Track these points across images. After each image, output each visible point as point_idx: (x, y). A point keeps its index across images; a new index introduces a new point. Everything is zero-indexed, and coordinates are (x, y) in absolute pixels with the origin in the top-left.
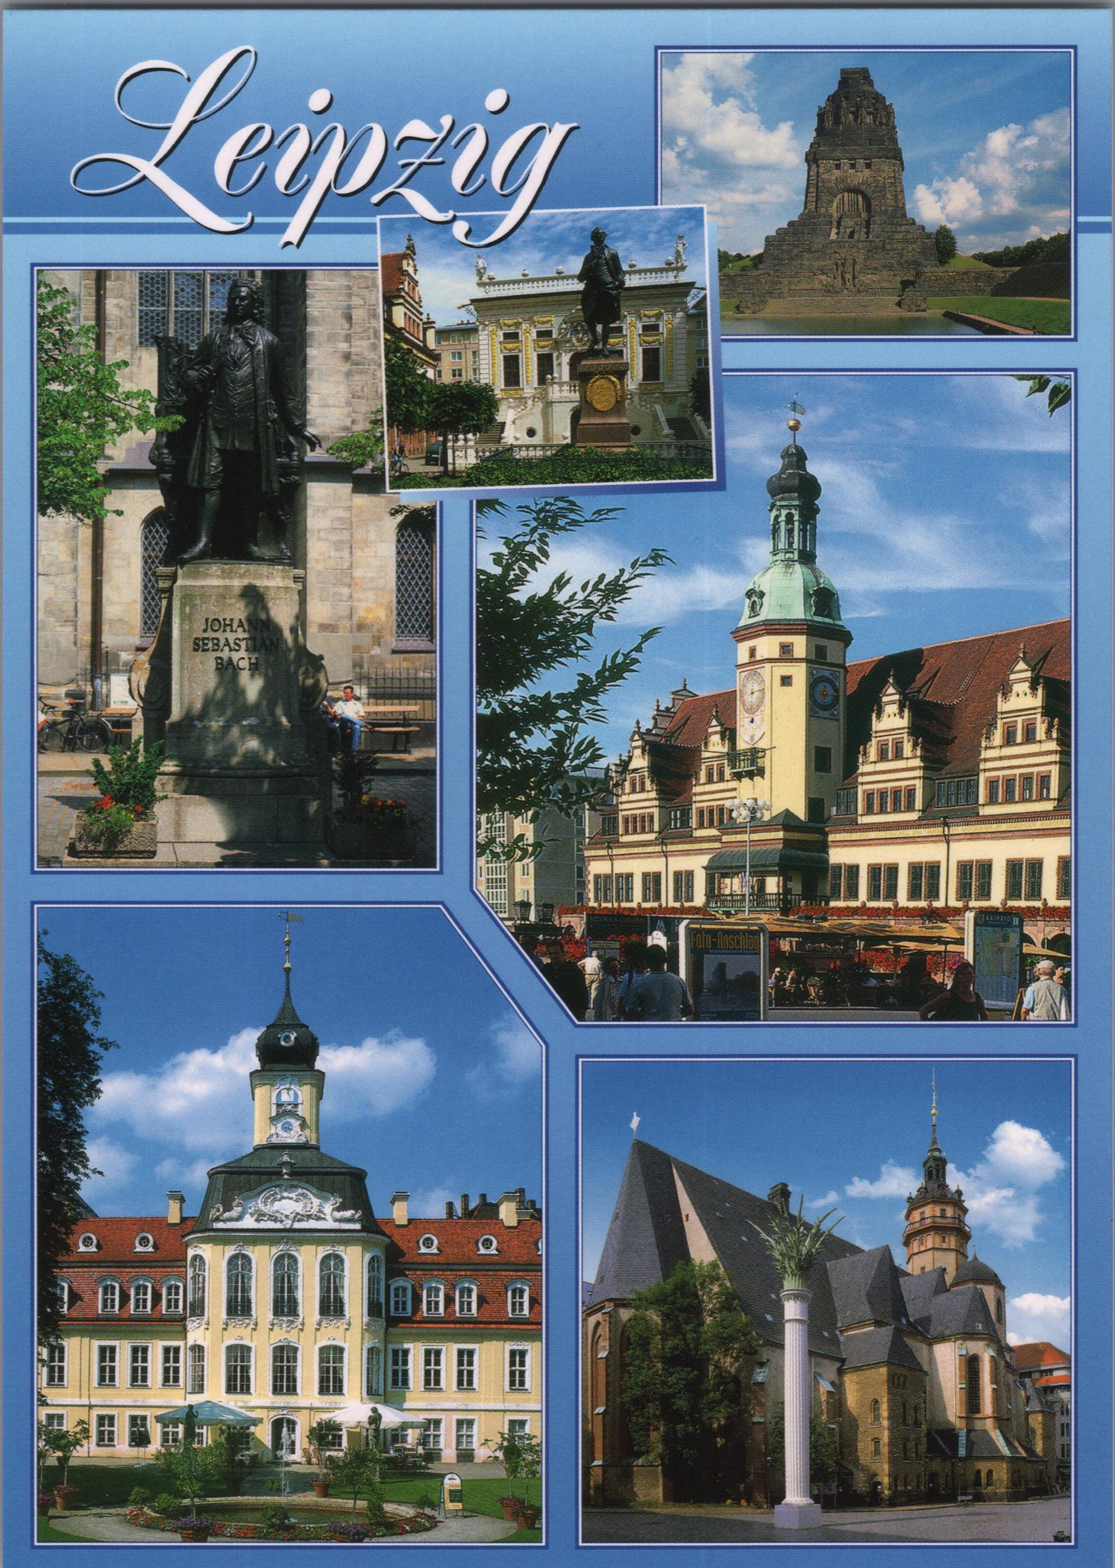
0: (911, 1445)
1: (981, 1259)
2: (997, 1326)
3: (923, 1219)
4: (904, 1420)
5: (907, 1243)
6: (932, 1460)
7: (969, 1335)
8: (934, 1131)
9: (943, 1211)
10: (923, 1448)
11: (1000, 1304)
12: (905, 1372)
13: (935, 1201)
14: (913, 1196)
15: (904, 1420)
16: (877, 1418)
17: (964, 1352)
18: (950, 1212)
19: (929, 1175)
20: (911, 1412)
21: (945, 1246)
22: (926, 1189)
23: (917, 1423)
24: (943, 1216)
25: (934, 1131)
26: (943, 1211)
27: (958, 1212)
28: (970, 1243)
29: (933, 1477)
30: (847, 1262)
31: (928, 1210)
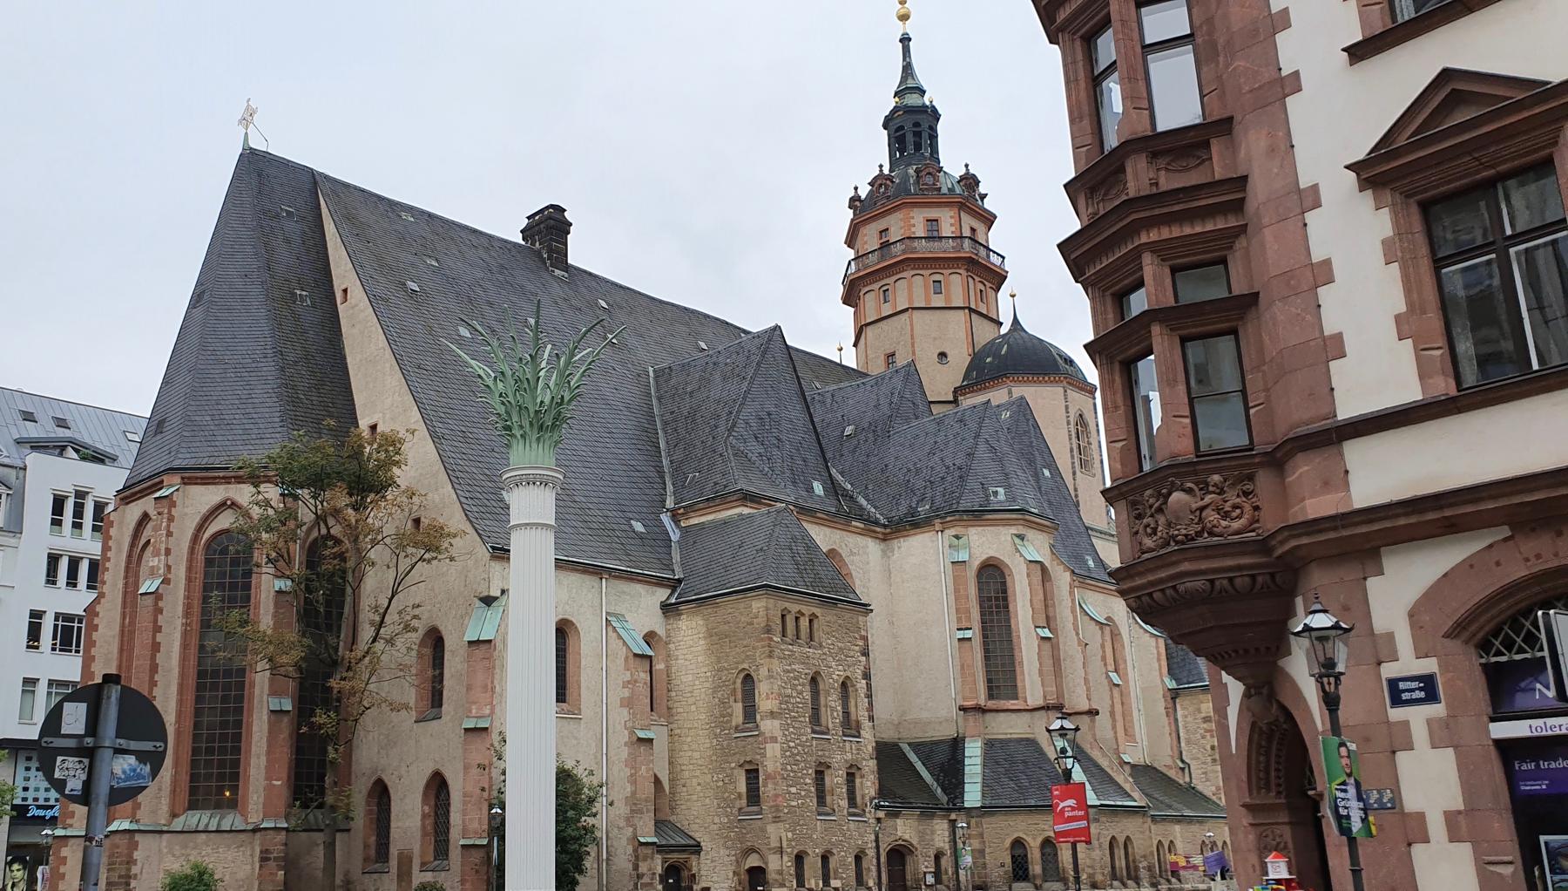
0: (836, 779)
1: (1032, 327)
3: (885, 245)
4: (815, 718)
5: (850, 298)
15: (815, 718)
16: (750, 712)
20: (832, 701)
21: (938, 301)
23: (850, 727)
28: (1003, 294)
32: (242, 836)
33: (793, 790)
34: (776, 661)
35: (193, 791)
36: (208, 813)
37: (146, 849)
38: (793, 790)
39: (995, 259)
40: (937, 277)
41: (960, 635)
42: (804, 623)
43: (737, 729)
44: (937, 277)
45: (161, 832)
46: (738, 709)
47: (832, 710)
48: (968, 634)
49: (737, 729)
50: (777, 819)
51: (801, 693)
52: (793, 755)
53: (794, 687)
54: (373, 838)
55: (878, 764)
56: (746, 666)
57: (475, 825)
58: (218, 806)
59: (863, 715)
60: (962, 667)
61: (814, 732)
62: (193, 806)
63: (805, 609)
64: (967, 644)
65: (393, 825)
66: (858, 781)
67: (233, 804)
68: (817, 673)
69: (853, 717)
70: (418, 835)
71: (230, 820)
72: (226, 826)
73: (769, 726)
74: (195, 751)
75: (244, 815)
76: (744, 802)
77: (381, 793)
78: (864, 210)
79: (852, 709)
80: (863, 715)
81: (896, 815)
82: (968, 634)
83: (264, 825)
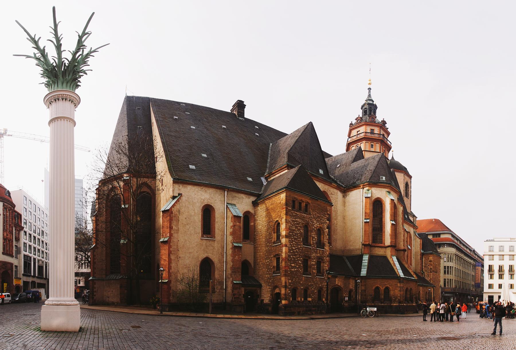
1: (396, 159)
2: (405, 199)
6: (335, 277)
7: (374, 183)
8: (370, 92)
9: (372, 130)
10: (326, 266)
11: (407, 186)
12: (305, 199)
13: (367, 124)
14: (353, 123)
16: (279, 236)
17: (369, 195)
18: (377, 130)
19: (365, 112)
20: (314, 234)
21: (373, 150)
22: (361, 118)
23: (320, 244)
24: (372, 132)
25: (370, 92)
26: (372, 130)
27: (382, 132)
29: (337, 290)
30: (285, 137)
31: (362, 129)
33: (293, 265)
34: (289, 217)
38: (293, 265)
39: (388, 142)
40: (372, 144)
41: (365, 221)
42: (303, 205)
43: (274, 243)
44: (372, 144)
46: (275, 236)
47: (313, 238)
48: (368, 220)
49: (274, 243)
50: (285, 275)
51: (300, 230)
52: (294, 252)
53: (296, 227)
55: (330, 259)
56: (278, 219)
59: (326, 241)
60: (365, 231)
61: (304, 245)
63: (303, 199)
64: (367, 224)
66: (322, 264)
68: (308, 223)
69: (322, 242)
73: (284, 241)
76: (275, 269)
78: (352, 127)
79: (322, 239)
80: (326, 241)
81: (336, 277)
82: (368, 220)
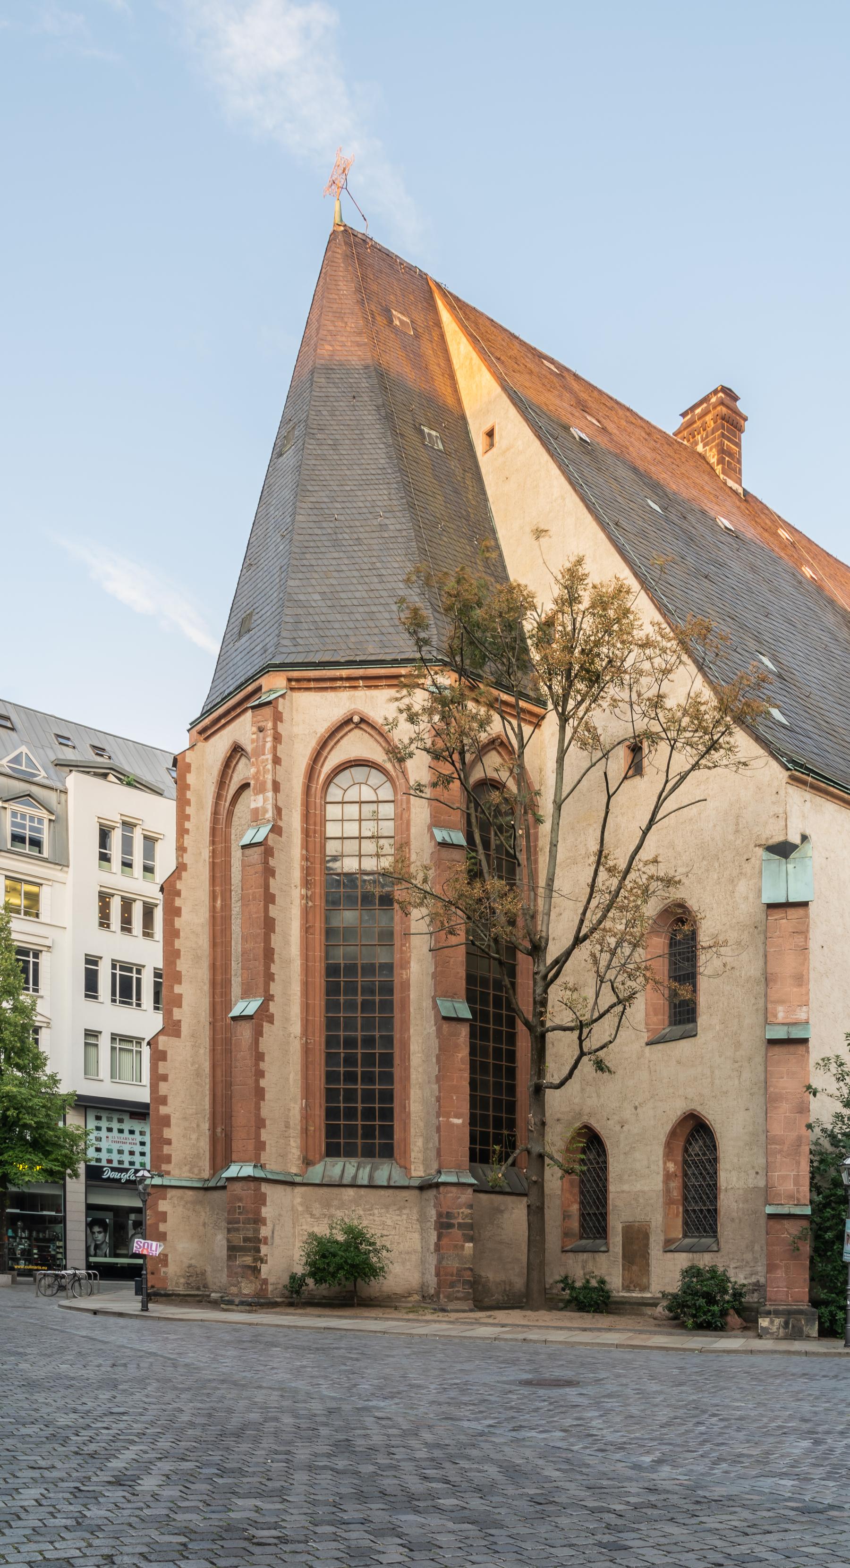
32: (405, 1194)
35: (332, 1131)
36: (354, 1161)
37: (278, 1205)
45: (293, 1184)
54: (575, 1208)
57: (790, 1186)
58: (369, 1153)
62: (332, 1151)
65: (612, 1188)
67: (387, 1152)
70: (659, 1202)
71: (384, 1172)
72: (381, 1177)
74: (331, 1077)
75: (406, 1168)
77: (591, 1142)
83: (443, 1179)
